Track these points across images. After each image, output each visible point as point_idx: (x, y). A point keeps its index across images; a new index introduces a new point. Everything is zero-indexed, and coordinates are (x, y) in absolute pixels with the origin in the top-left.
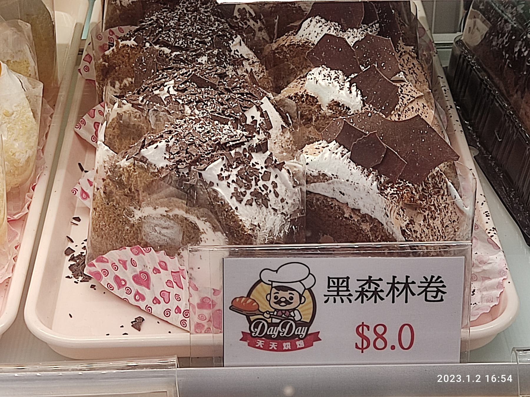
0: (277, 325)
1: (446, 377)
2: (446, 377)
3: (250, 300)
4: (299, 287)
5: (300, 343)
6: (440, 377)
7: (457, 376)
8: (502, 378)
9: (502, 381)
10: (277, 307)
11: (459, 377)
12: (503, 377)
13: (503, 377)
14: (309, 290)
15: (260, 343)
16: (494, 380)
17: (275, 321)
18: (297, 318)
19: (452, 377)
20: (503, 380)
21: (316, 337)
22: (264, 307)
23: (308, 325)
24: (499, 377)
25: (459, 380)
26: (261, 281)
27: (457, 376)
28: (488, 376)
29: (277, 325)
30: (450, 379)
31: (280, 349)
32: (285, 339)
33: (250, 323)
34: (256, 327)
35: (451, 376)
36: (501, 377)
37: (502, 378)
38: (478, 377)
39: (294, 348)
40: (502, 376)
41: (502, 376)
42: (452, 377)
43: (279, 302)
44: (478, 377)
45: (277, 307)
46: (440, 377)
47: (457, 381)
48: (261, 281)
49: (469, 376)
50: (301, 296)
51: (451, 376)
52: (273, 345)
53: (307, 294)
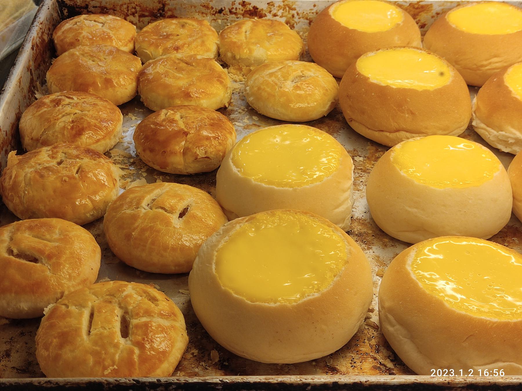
1: (439, 371)
2: (439, 371)
6: (433, 371)
7: (450, 370)
8: (494, 372)
9: (494, 375)
11: (452, 371)
12: (496, 371)
13: (496, 371)
16: (486, 374)
19: (446, 371)
20: (496, 374)
24: (491, 372)
25: (452, 374)
27: (450, 370)
28: (480, 370)
30: (443, 373)
35: (444, 371)
36: (493, 371)
37: (494, 372)
38: (471, 371)
40: (495, 370)
41: (495, 370)
42: (446, 371)
44: (471, 371)
46: (433, 371)
47: (450, 375)
49: (461, 370)
51: (444, 371)
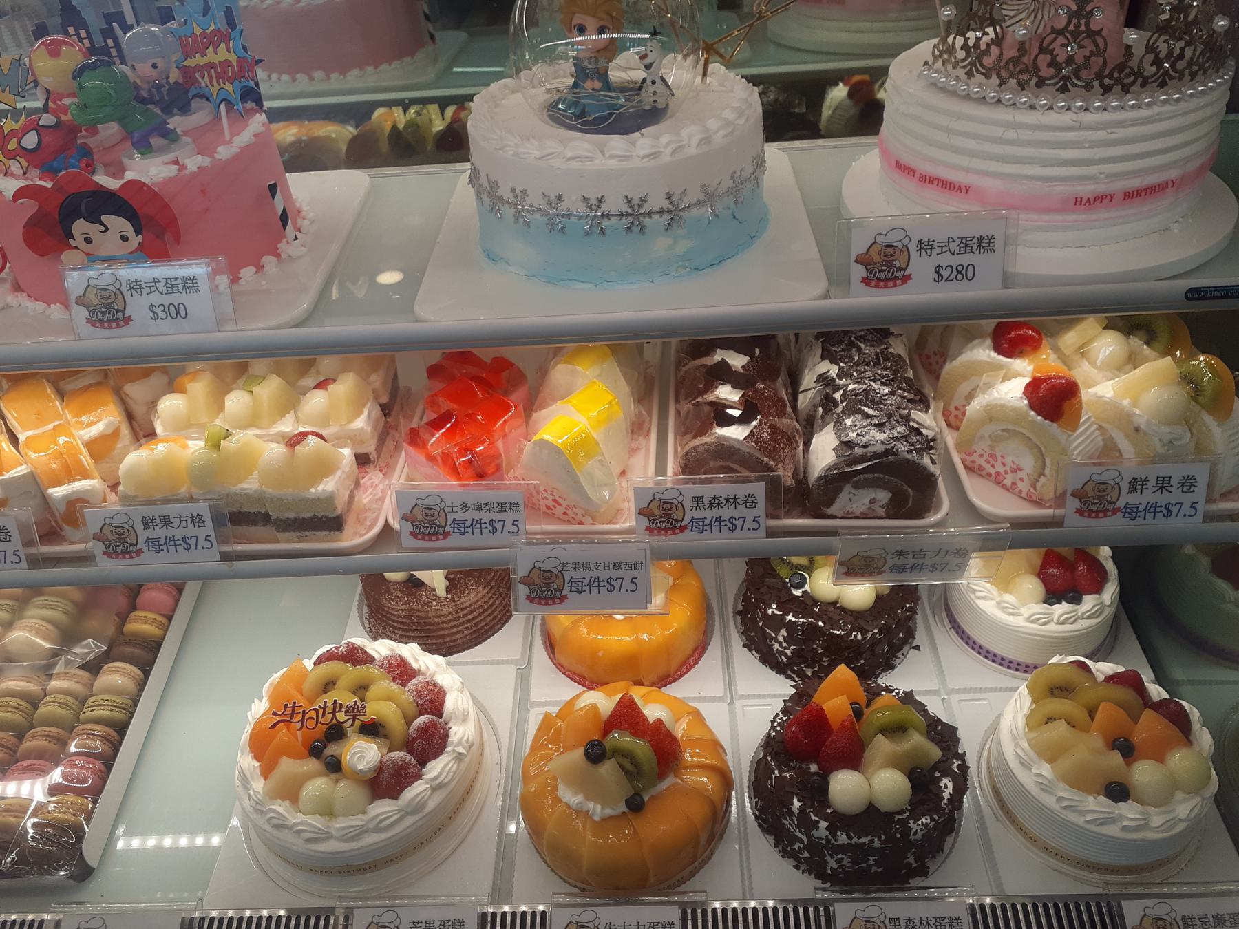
0: (885, 271)
3: (867, 256)
4: (899, 245)
5: (899, 282)
10: (886, 259)
14: (906, 246)
15: (873, 284)
17: (883, 268)
18: (898, 265)
21: (909, 277)
22: (877, 259)
23: (904, 269)
26: (875, 242)
29: (885, 271)
31: (886, 287)
32: (889, 280)
33: (867, 270)
34: (871, 273)
39: (895, 285)
43: (886, 256)
45: (886, 259)
48: (875, 242)
50: (900, 250)
52: (882, 284)
53: (905, 249)
